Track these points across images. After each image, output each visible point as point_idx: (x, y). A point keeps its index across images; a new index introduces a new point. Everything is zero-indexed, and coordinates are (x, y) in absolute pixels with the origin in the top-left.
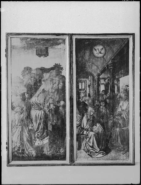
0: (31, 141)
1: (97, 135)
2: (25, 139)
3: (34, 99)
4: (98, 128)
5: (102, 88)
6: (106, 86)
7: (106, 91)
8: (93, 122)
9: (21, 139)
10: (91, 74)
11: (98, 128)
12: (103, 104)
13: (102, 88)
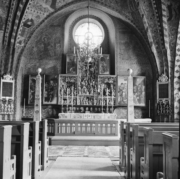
0: (123, 100)
1: (138, 100)
2: (121, 100)
3: (123, 91)
4: (138, 98)
5: (139, 88)
6: (140, 88)
7: (140, 89)
8: (137, 96)
9: (120, 100)
10: (136, 85)
11: (138, 98)
12: (139, 92)
13: (139, 88)
